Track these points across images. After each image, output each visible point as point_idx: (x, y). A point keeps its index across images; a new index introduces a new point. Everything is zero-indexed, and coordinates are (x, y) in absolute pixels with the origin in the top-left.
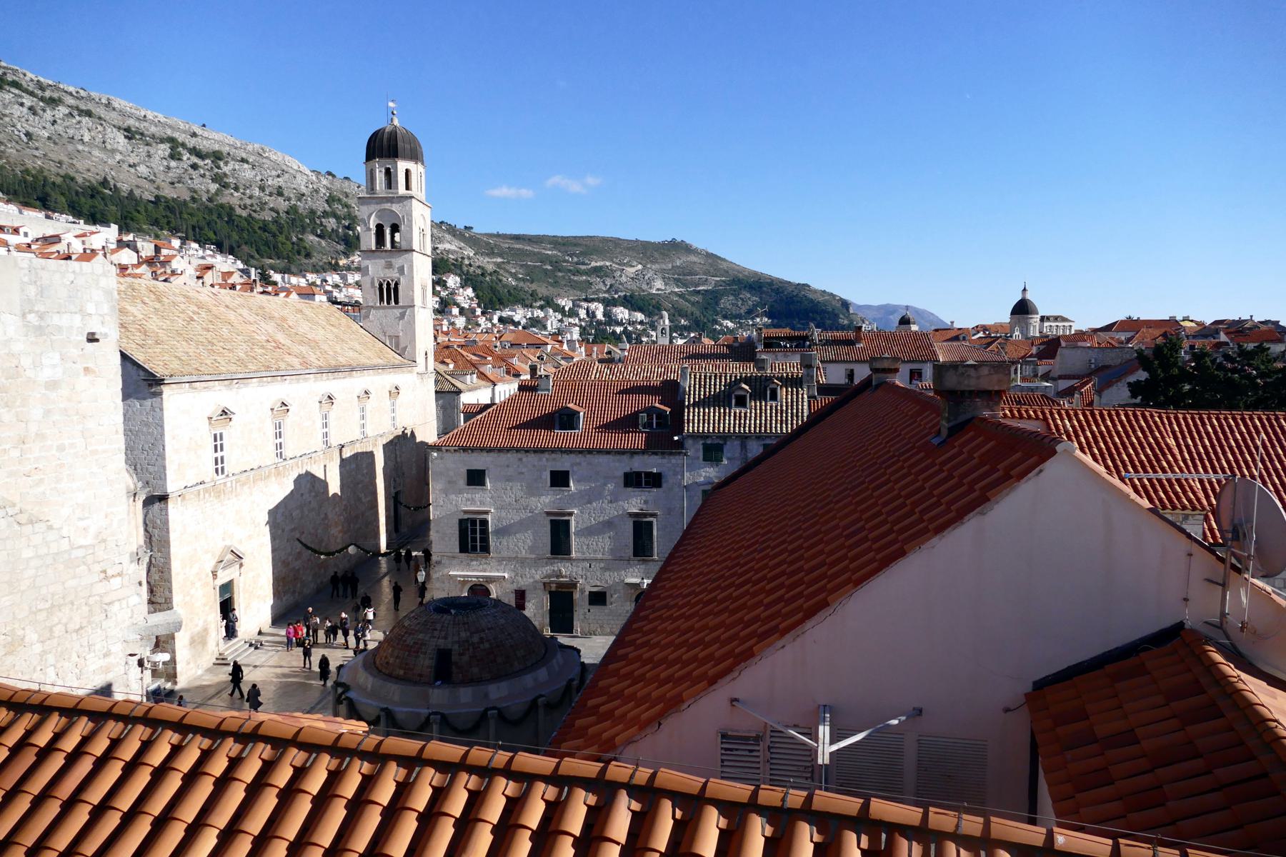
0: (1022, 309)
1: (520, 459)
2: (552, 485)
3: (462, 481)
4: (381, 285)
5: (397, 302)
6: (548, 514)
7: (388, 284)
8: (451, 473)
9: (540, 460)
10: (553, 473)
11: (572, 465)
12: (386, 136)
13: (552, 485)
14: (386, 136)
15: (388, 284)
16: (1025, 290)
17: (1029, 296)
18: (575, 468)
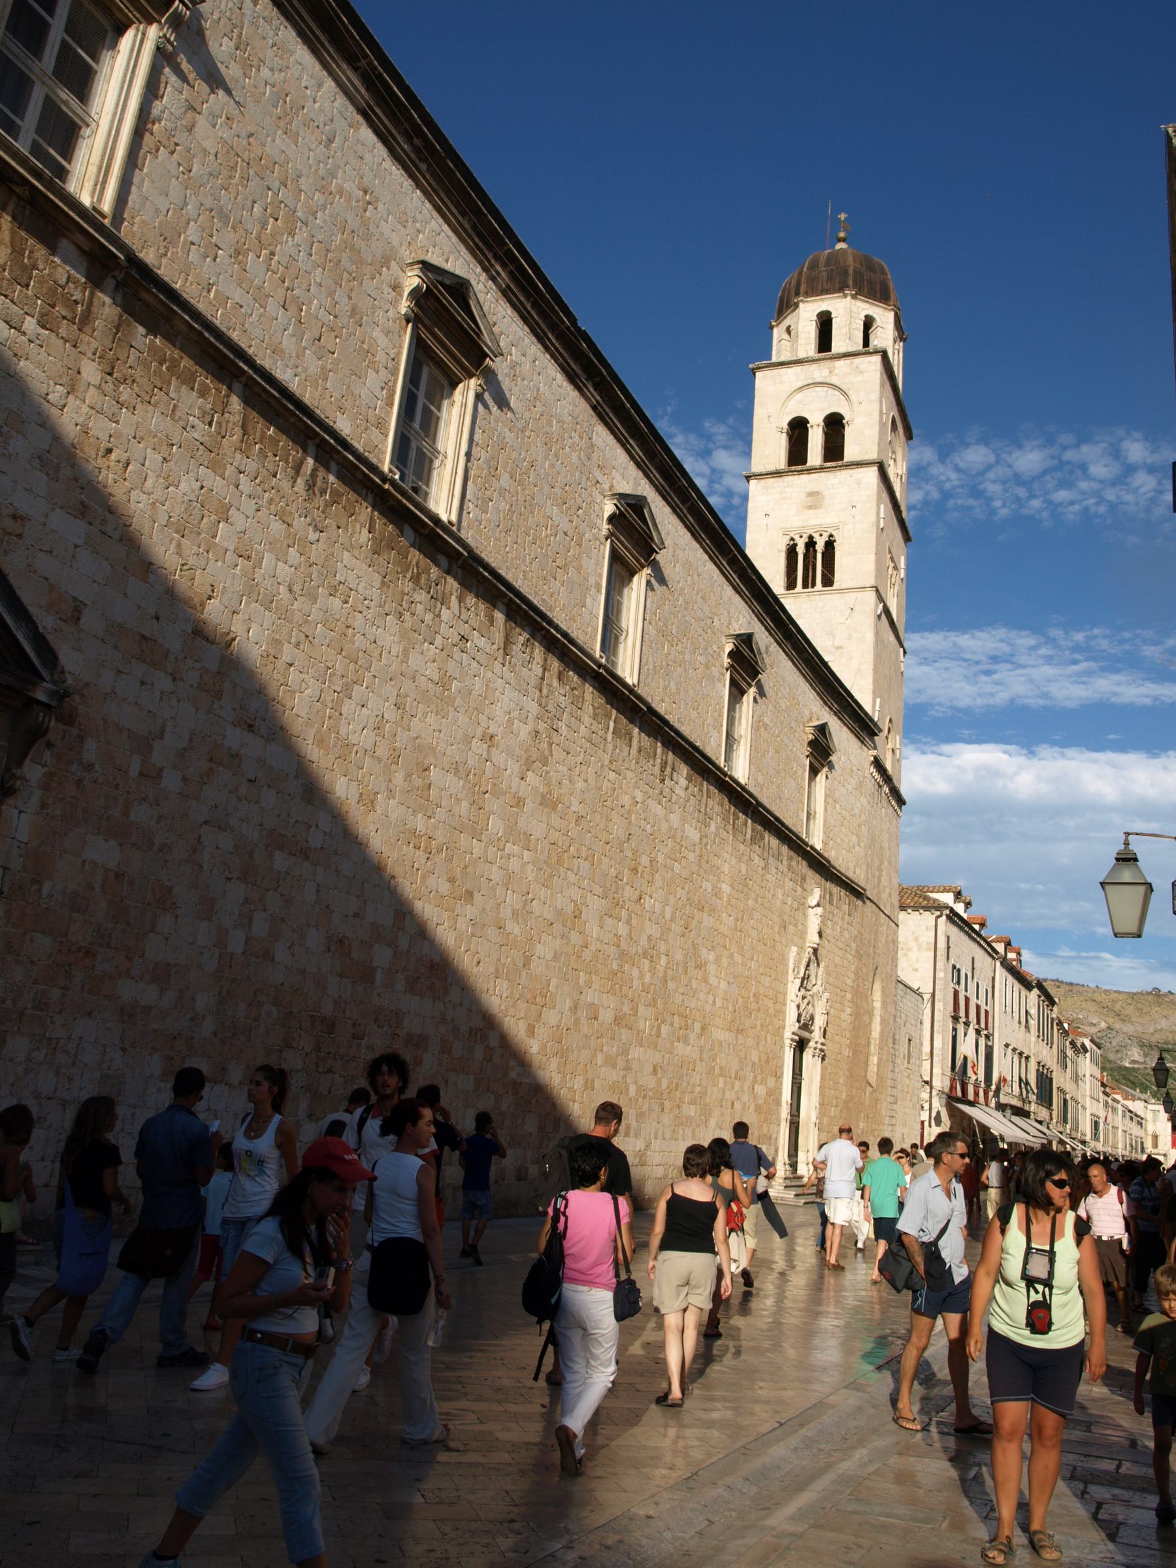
4: (791, 552)
5: (828, 581)
7: (811, 544)
15: (811, 544)
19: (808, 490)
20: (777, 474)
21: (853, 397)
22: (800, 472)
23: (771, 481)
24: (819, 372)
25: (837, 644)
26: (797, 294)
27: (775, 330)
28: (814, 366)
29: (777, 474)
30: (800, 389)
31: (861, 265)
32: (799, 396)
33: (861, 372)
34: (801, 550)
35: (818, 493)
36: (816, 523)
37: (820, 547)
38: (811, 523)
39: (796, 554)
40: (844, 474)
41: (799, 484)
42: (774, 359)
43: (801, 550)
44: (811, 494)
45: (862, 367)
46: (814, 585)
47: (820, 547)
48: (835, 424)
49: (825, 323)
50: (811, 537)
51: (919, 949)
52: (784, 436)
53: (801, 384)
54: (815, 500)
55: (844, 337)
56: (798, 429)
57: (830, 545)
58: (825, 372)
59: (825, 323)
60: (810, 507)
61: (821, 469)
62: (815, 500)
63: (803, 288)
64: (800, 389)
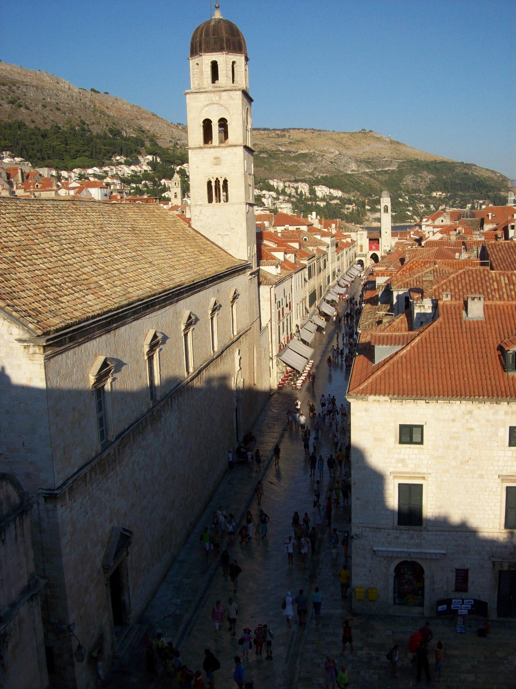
1: (470, 412)
4: (209, 183)
7: (217, 181)
19: (214, 156)
20: (201, 148)
22: (210, 148)
24: (214, 97)
25: (232, 227)
26: (201, 51)
27: (191, 61)
28: (212, 94)
29: (201, 148)
30: (207, 106)
31: (229, 34)
32: (207, 108)
33: (233, 99)
34: (213, 184)
37: (221, 184)
39: (211, 187)
40: (229, 149)
41: (210, 153)
42: (193, 90)
43: (213, 184)
44: (216, 158)
45: (233, 96)
46: (220, 201)
47: (221, 184)
48: (223, 123)
49: (214, 66)
50: (217, 179)
51: (264, 301)
52: (202, 128)
53: (207, 103)
54: (217, 161)
55: (223, 71)
56: (207, 124)
57: (225, 181)
58: (218, 98)
59: (214, 66)
60: (216, 164)
61: (219, 147)
62: (217, 161)
63: (203, 47)
64: (207, 106)
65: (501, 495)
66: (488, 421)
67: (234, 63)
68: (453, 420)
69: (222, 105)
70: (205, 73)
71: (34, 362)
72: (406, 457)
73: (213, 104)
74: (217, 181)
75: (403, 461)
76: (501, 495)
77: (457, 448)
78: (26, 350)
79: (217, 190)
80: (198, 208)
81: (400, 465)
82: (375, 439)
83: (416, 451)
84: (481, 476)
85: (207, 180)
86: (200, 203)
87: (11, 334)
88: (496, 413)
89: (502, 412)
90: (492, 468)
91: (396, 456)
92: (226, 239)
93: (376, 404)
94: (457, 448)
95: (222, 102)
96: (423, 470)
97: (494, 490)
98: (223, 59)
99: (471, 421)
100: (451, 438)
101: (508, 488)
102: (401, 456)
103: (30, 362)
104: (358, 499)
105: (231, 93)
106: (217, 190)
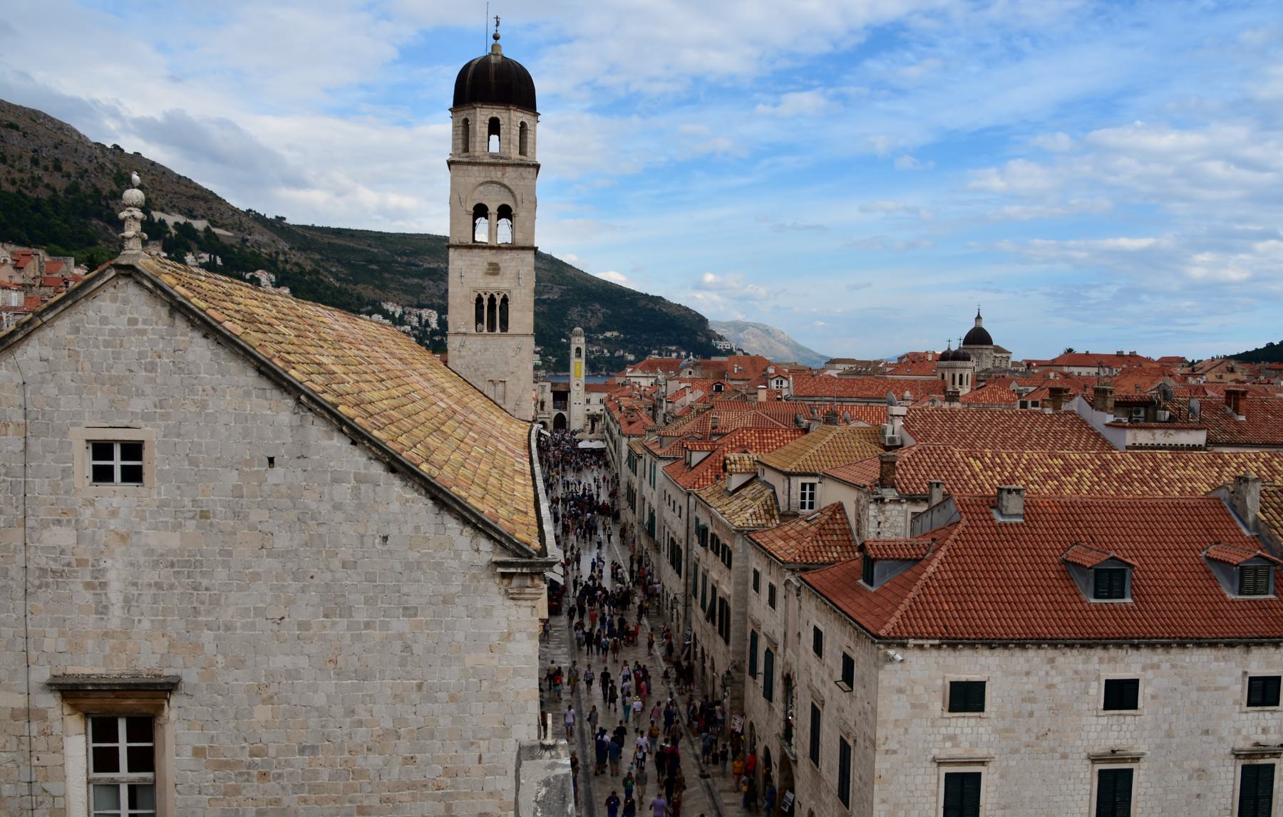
0: (978, 337)
1: (1052, 661)
2: (1107, 707)
3: (938, 704)
4: (479, 300)
5: (505, 325)
6: (1094, 759)
7: (492, 299)
8: (919, 689)
9: (1086, 662)
10: (1110, 685)
11: (1144, 669)
12: (492, 70)
13: (1106, 707)
14: (492, 70)
15: (492, 299)
16: (979, 317)
17: (985, 325)
18: (1150, 674)
21: (518, 197)
23: (464, 251)
24: (496, 174)
30: (482, 184)
34: (486, 303)
35: (496, 264)
36: (496, 285)
37: (498, 303)
38: (493, 285)
39: (482, 307)
43: (486, 303)
44: (491, 264)
45: (524, 174)
47: (498, 303)
53: (482, 180)
57: (505, 300)
58: (499, 174)
62: (494, 269)
64: (482, 184)
65: (1091, 784)
66: (1076, 672)
67: (523, 124)
68: (1027, 674)
69: (505, 186)
70: (478, 134)
71: (519, 603)
72: (958, 731)
73: (492, 182)
74: (492, 299)
75: (952, 738)
76: (1091, 784)
77: (1031, 714)
78: (506, 582)
79: (492, 312)
80: (459, 338)
81: (948, 744)
82: (914, 706)
83: (973, 721)
84: (1064, 756)
85: (476, 295)
86: (463, 330)
87: (478, 550)
88: (1086, 662)
89: (1096, 659)
90: (1079, 743)
91: (943, 730)
92: (500, 387)
93: (917, 652)
94: (1031, 714)
95: (506, 181)
96: (980, 753)
97: (1082, 776)
98: (512, 118)
99: (1053, 673)
100: (1023, 700)
101: (1101, 772)
102: (951, 731)
103: (512, 603)
104: (883, 801)
105: (521, 169)
106: (492, 312)
